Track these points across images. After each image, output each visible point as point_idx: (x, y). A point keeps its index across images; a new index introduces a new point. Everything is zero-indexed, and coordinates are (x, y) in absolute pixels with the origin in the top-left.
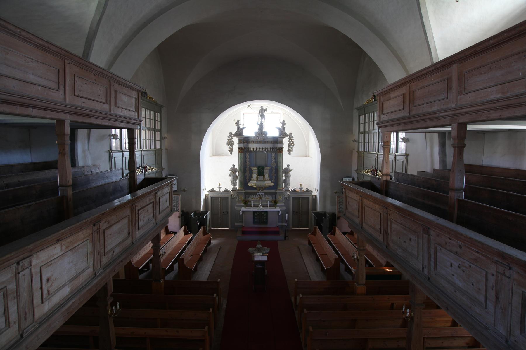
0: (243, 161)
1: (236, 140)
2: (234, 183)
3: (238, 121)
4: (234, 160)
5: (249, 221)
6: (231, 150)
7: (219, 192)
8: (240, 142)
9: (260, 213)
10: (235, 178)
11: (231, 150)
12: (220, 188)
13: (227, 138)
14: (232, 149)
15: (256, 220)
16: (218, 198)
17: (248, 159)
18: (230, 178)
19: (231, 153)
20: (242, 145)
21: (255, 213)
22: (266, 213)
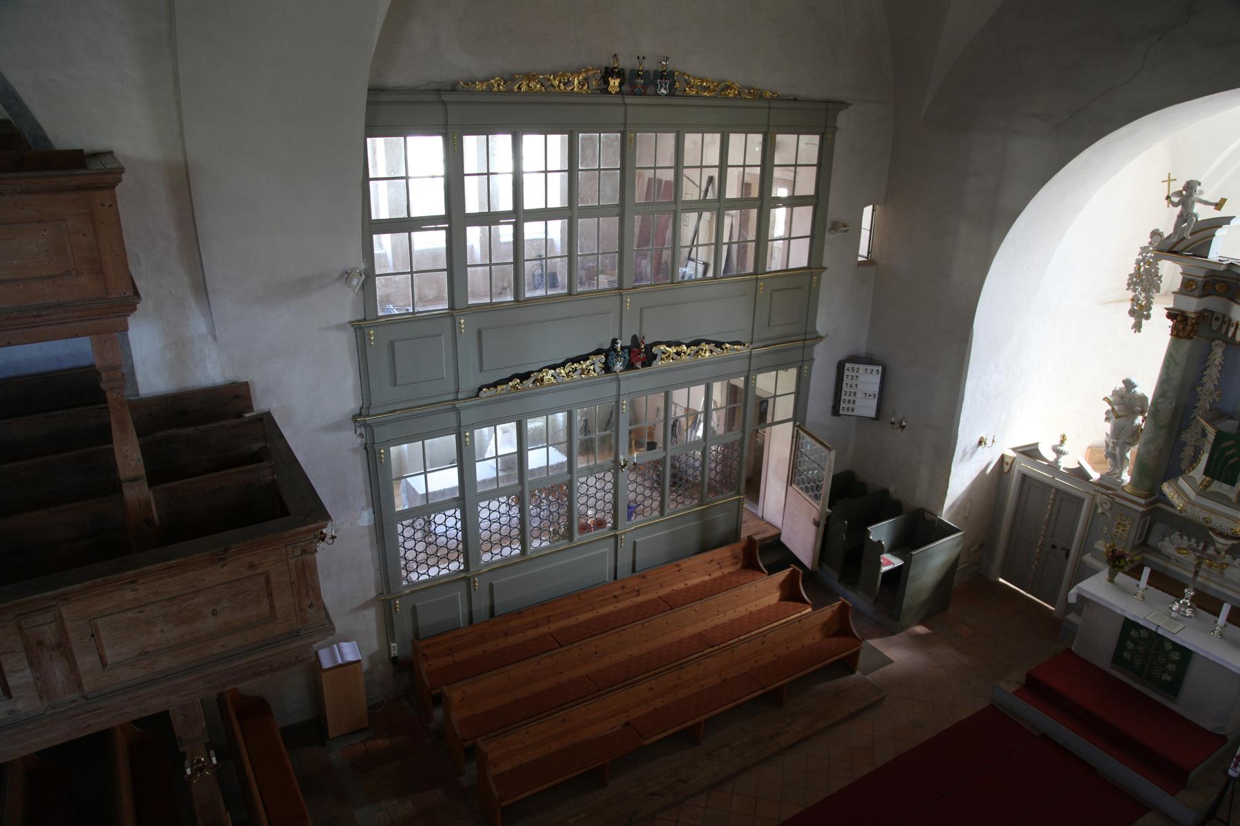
0: (1177, 375)
1: (1171, 273)
2: (1114, 454)
3: (1190, 186)
4: (1145, 356)
5: (1099, 648)
6: (1140, 313)
7: (1053, 467)
8: (1188, 286)
9: (1156, 640)
10: (1122, 436)
11: (1140, 313)
12: (1060, 453)
13: (1135, 255)
14: (1148, 307)
15: (1126, 655)
16: (1045, 486)
17: (1213, 373)
18: (1107, 427)
19: (1137, 327)
20: (1191, 305)
21: (1129, 625)
22: (1186, 654)
